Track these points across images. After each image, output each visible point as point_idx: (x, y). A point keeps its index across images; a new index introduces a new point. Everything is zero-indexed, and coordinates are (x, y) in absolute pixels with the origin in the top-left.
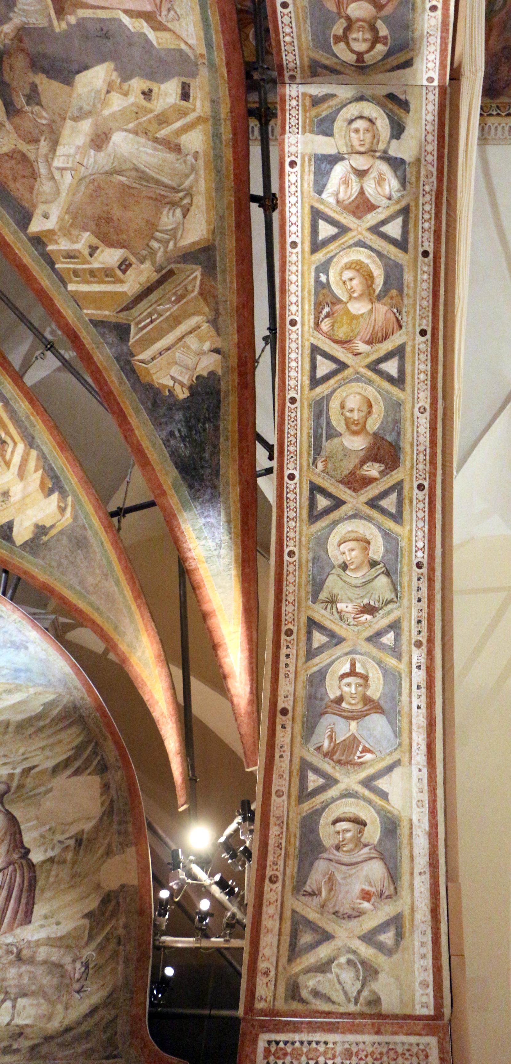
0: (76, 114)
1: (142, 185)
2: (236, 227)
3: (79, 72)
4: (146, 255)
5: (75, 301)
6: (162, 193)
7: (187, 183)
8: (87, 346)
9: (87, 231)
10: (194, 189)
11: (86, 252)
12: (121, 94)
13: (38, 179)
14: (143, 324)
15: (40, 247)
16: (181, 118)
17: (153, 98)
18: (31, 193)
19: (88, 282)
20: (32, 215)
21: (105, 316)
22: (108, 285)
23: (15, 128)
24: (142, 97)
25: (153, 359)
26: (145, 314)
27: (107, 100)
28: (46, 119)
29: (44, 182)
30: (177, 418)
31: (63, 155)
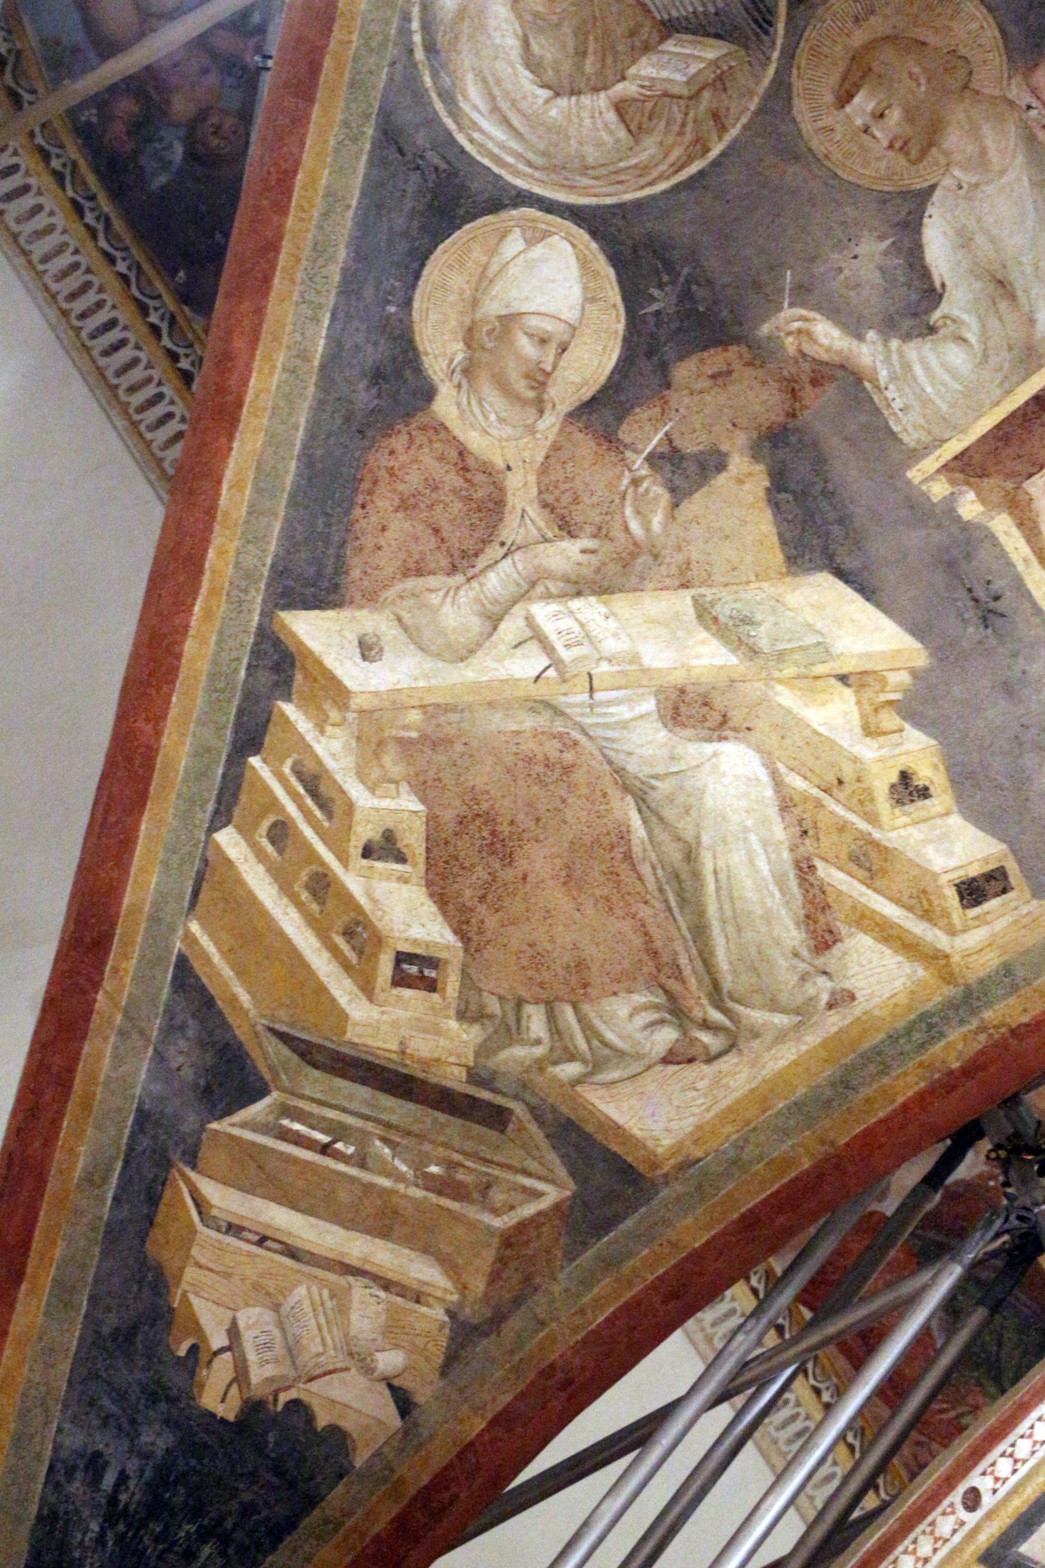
0: (723, 611)
1: (661, 890)
2: (743, 1216)
3: (841, 574)
4: (491, 1017)
5: (200, 879)
6: (683, 961)
7: (756, 1016)
8: (100, 996)
9: (423, 800)
10: (756, 1044)
11: (365, 831)
12: (863, 716)
13: (459, 578)
14: (297, 1126)
15: (265, 678)
16: (910, 909)
17: (910, 808)
18: (406, 573)
19: (286, 889)
20: (337, 605)
21: (234, 999)
22: (326, 955)
23: (556, 447)
24: (894, 778)
25: (233, 1229)
26: (331, 1114)
27: (820, 684)
28: (648, 530)
29: (463, 597)
30: (146, 1438)
31: (582, 625)
